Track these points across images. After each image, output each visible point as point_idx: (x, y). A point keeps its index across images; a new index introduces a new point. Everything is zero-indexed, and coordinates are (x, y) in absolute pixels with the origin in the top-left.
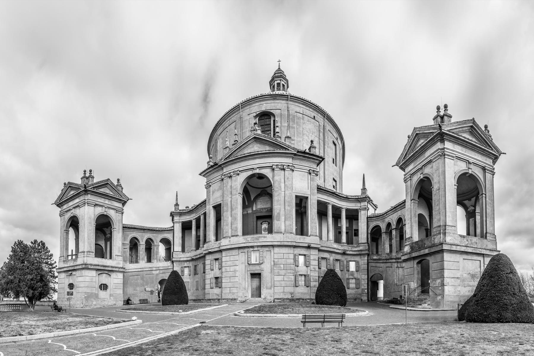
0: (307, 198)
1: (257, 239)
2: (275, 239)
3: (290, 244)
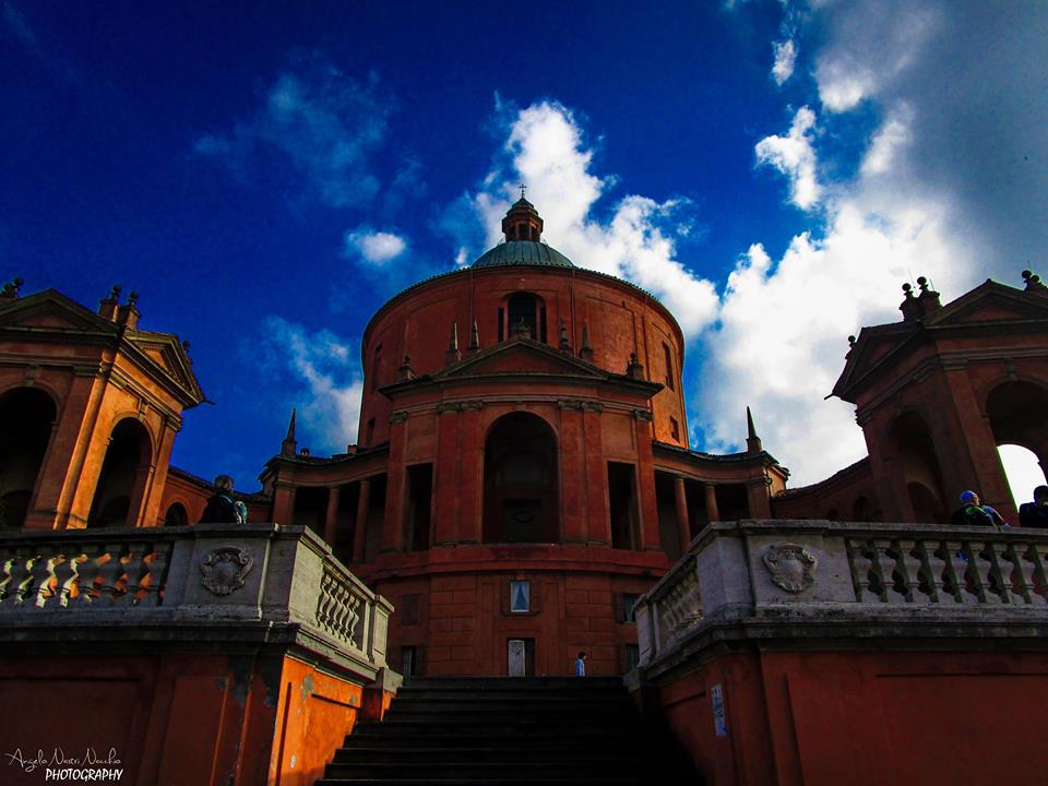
0: (633, 466)
3: (601, 568)
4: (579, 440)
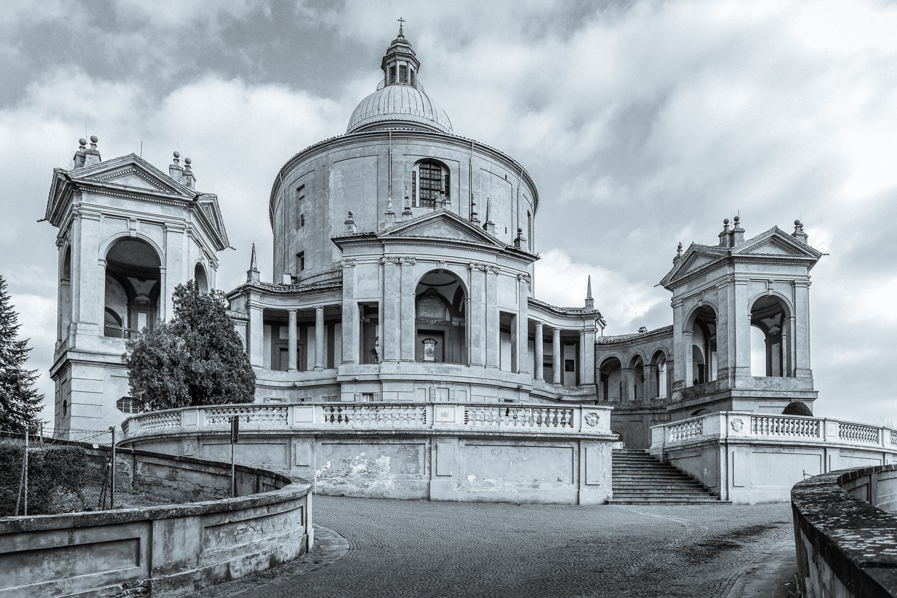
1: (447, 370)
2: (473, 375)
3: (494, 383)
4: (483, 294)
